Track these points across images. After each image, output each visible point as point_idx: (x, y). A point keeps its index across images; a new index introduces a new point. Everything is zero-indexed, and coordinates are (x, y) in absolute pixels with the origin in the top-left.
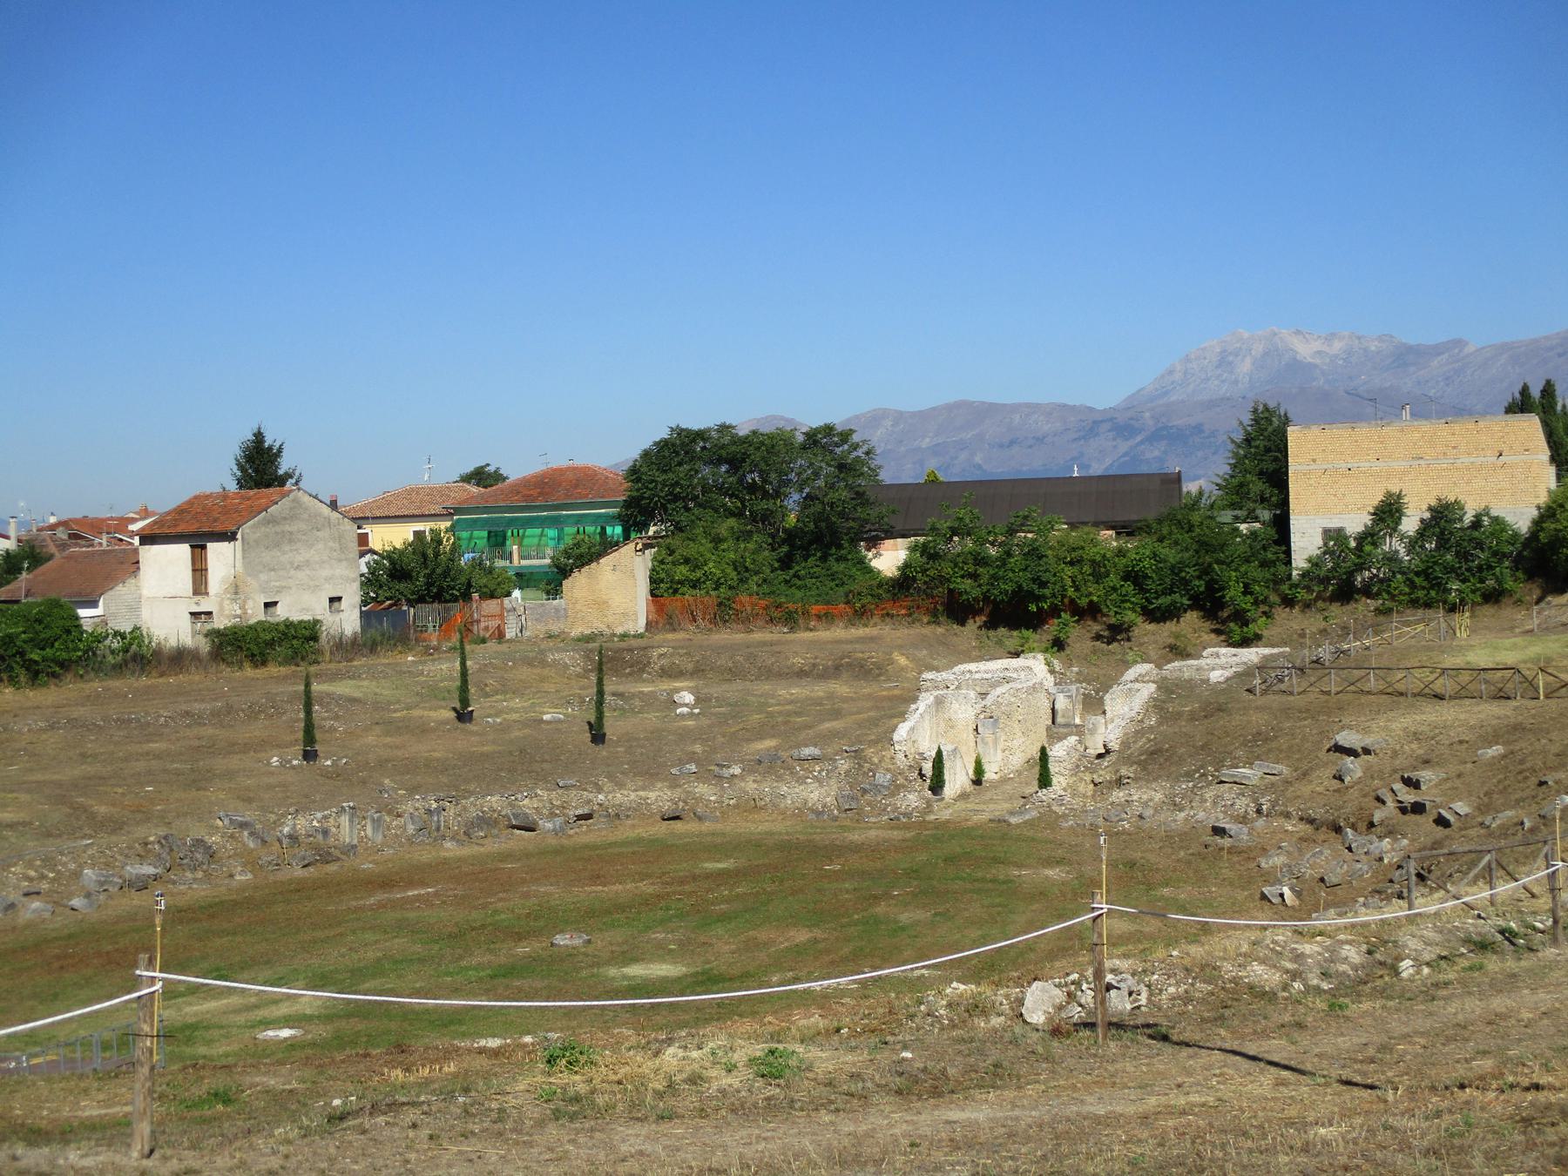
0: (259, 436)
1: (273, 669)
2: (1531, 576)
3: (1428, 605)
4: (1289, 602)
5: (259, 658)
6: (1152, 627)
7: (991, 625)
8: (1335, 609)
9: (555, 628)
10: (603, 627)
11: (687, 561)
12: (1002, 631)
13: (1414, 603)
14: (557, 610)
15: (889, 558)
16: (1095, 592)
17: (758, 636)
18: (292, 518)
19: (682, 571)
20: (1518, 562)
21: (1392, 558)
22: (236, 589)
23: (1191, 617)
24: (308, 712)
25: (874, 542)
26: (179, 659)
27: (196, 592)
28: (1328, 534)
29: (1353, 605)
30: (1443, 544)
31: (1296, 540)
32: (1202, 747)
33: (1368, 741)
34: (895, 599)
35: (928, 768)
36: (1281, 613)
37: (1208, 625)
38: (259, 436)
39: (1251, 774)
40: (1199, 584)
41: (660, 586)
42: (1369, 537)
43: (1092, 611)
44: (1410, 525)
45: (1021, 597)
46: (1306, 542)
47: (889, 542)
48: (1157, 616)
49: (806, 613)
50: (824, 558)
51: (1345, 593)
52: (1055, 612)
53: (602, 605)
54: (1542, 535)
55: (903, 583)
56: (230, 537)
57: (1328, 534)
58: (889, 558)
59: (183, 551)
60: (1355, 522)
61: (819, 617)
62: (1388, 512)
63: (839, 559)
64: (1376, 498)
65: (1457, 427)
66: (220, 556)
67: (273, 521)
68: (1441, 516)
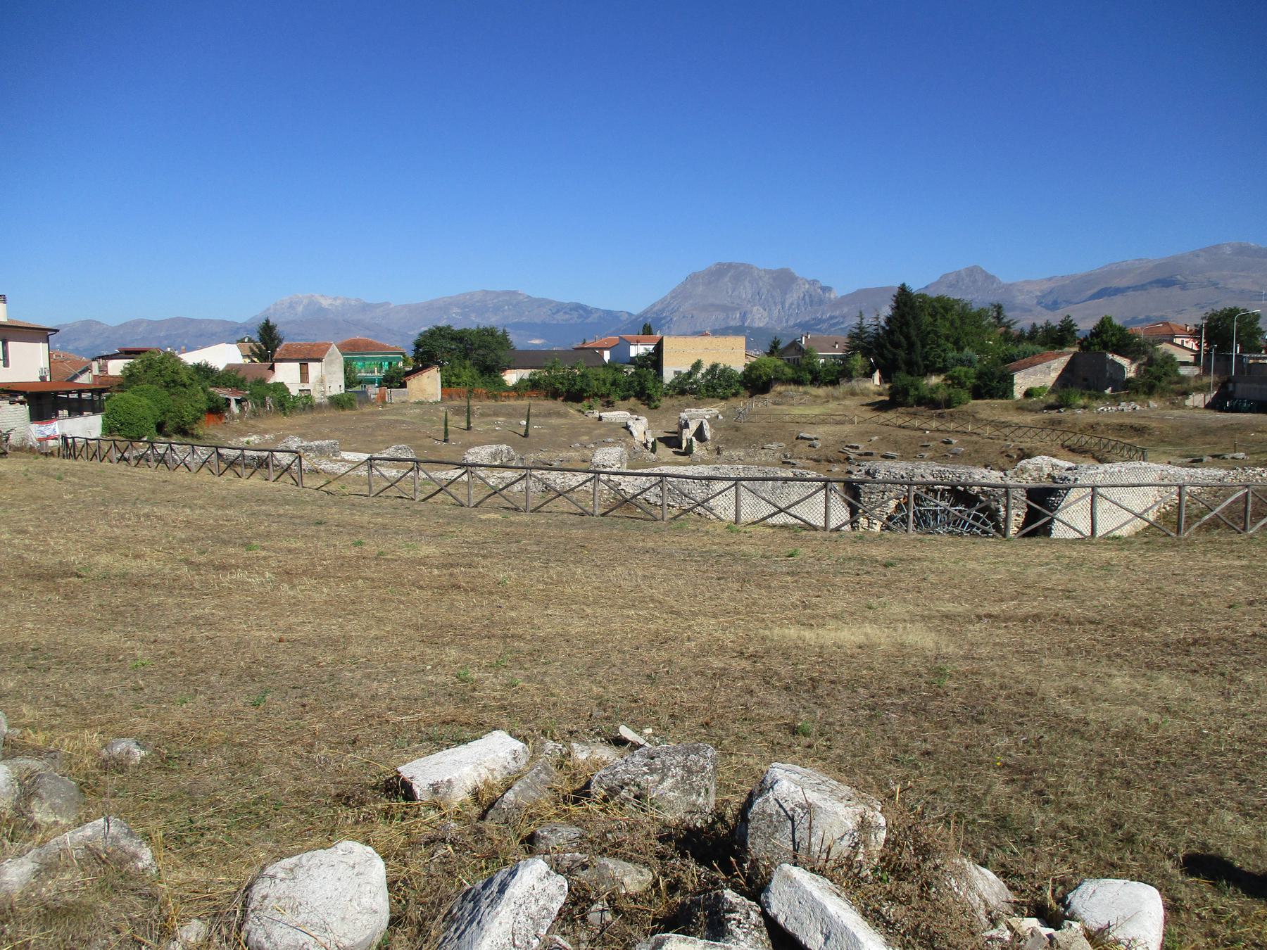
0: (268, 321)
1: (347, 412)
2: (747, 388)
3: (713, 397)
4: (666, 395)
5: (343, 408)
6: (620, 402)
7: (566, 400)
8: (680, 397)
9: (404, 399)
10: (423, 399)
11: (456, 375)
12: (570, 403)
13: (708, 396)
14: (404, 392)
15: (511, 377)
16: (604, 390)
17: (484, 403)
18: (333, 354)
19: (453, 379)
20: (742, 383)
21: (696, 382)
22: (322, 381)
23: (633, 400)
24: (446, 425)
25: (504, 370)
26: (320, 405)
27: (301, 382)
28: (675, 372)
29: (685, 397)
30: (713, 378)
31: (665, 374)
32: (745, 438)
33: (815, 436)
34: (532, 390)
35: (650, 445)
36: (663, 399)
37: (640, 402)
38: (268, 321)
39: (774, 446)
40: (638, 389)
41: (446, 383)
42: (690, 374)
43: (602, 396)
44: (703, 371)
45: (582, 391)
46: (668, 375)
47: (509, 371)
48: (624, 398)
49: (501, 395)
50: (490, 376)
51: (683, 392)
52: (588, 397)
53: (423, 391)
54: (753, 376)
55: (532, 386)
56: (319, 360)
57: (675, 372)
58: (511, 377)
59: (296, 365)
60: (685, 369)
61: (505, 397)
62: (697, 366)
63: (495, 376)
64: (694, 361)
65: (719, 339)
66: (314, 368)
67: (329, 355)
68: (714, 367)
